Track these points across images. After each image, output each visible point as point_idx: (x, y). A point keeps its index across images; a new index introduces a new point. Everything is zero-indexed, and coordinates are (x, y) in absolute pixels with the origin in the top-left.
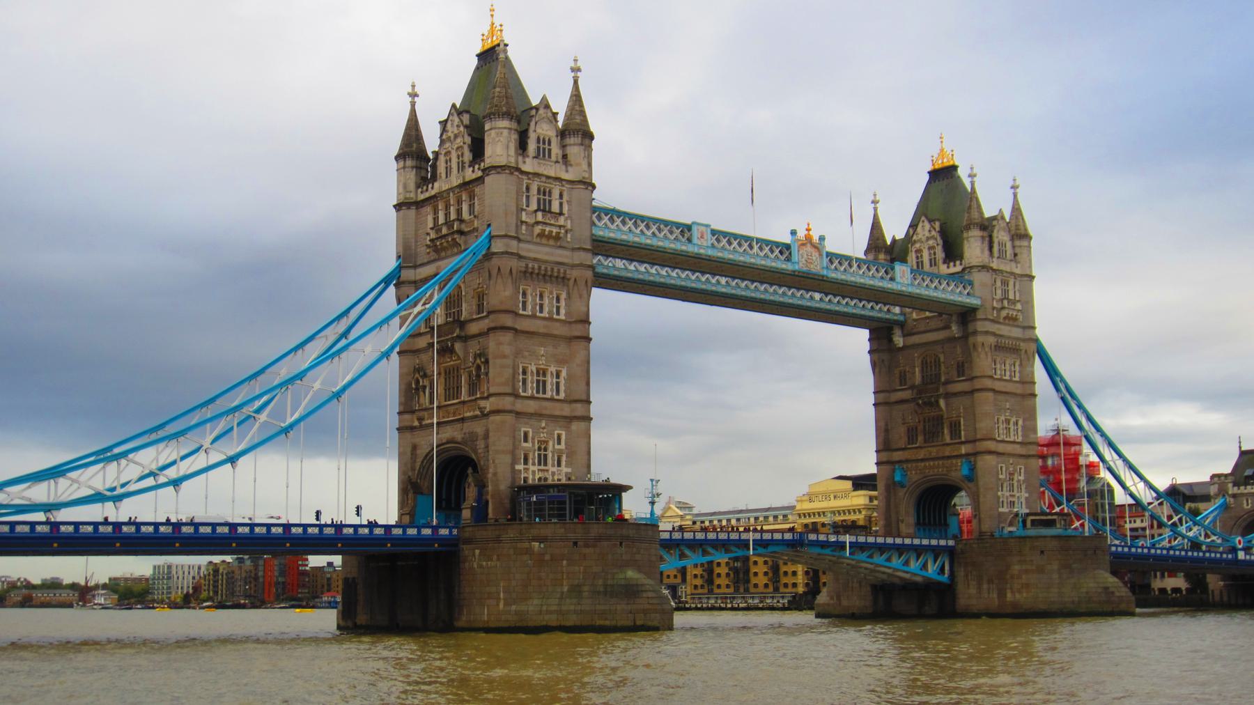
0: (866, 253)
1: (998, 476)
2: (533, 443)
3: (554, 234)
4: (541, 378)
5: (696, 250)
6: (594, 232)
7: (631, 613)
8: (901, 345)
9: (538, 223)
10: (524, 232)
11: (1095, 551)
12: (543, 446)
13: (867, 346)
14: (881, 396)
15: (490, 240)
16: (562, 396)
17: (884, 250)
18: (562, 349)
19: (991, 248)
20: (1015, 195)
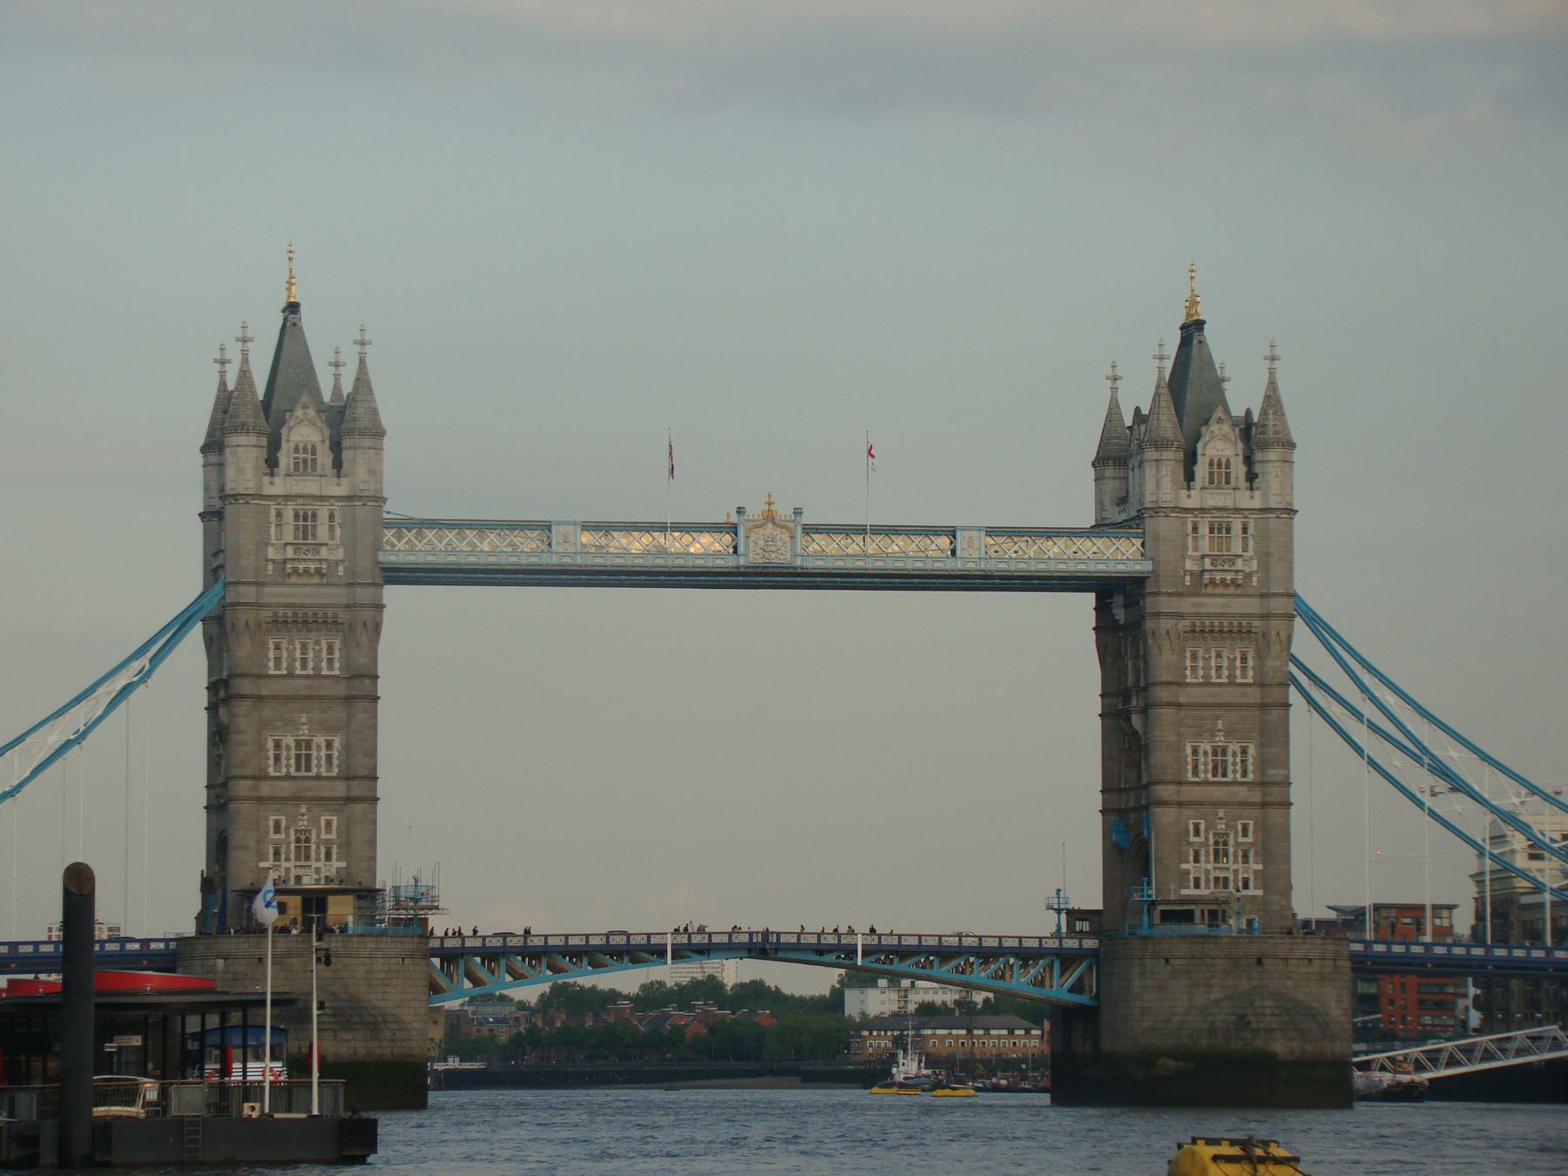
0: (1093, 465)
1: (1188, 841)
2: (288, 835)
3: (312, 571)
4: (304, 752)
5: (555, 560)
6: (381, 558)
7: (296, 1040)
8: (1122, 622)
9: (285, 561)
10: (270, 573)
11: (1259, 961)
12: (303, 840)
13: (1091, 619)
14: (1108, 700)
15: (224, 588)
16: (336, 771)
17: (1111, 463)
18: (338, 712)
19: (1189, 477)
20: (1272, 372)
